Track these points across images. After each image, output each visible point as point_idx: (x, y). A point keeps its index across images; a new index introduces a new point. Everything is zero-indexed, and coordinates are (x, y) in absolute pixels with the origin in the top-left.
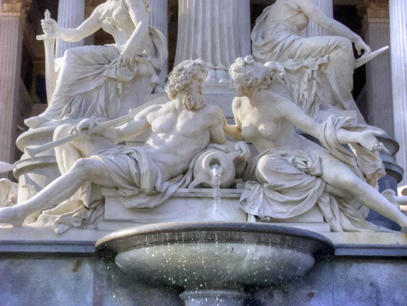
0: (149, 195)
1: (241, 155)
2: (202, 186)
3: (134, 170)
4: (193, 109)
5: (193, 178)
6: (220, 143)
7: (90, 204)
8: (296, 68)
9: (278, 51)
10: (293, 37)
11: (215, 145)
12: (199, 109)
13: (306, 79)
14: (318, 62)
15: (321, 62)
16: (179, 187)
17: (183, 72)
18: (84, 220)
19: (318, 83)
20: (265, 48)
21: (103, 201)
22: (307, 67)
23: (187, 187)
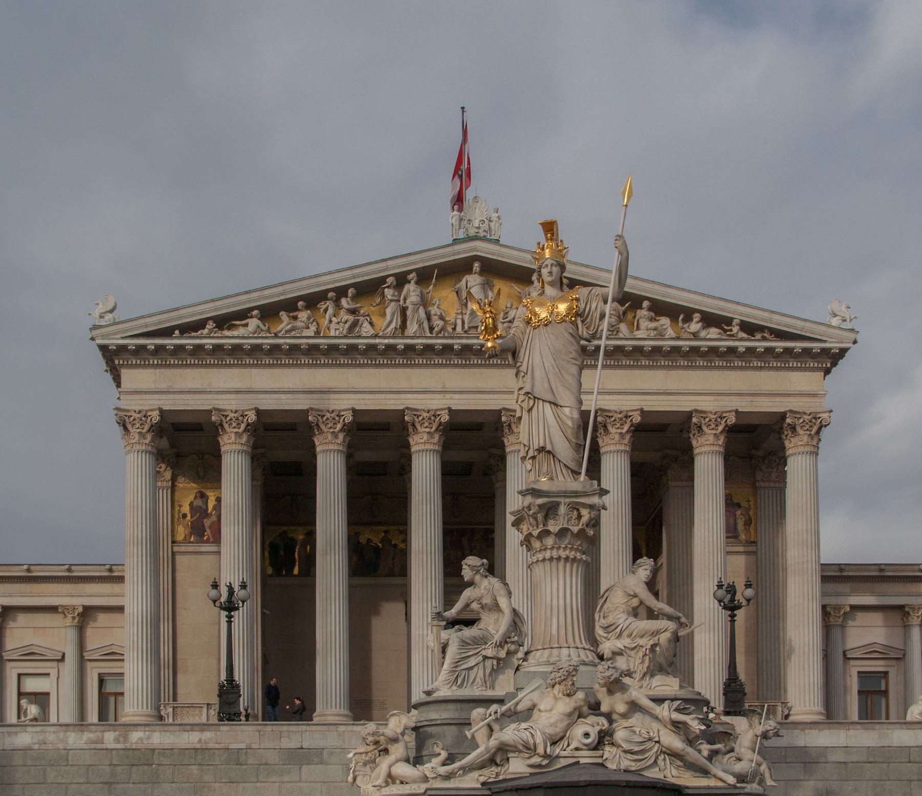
0: (541, 757)
1: (604, 728)
2: (577, 749)
3: (531, 742)
4: (569, 695)
5: (568, 745)
6: (585, 717)
7: (500, 762)
8: (634, 645)
9: (618, 633)
10: (631, 619)
11: (584, 720)
12: (572, 695)
13: (641, 654)
14: (651, 642)
15: (653, 643)
16: (561, 750)
17: (563, 670)
18: (497, 773)
19: (650, 658)
20: (607, 629)
21: (508, 759)
22: (642, 646)
23: (565, 750)
